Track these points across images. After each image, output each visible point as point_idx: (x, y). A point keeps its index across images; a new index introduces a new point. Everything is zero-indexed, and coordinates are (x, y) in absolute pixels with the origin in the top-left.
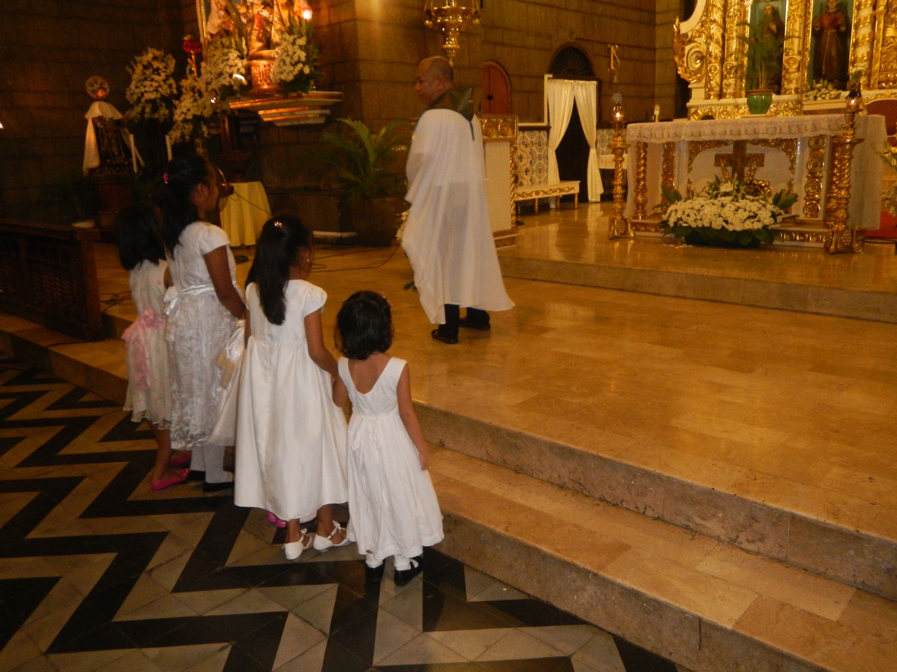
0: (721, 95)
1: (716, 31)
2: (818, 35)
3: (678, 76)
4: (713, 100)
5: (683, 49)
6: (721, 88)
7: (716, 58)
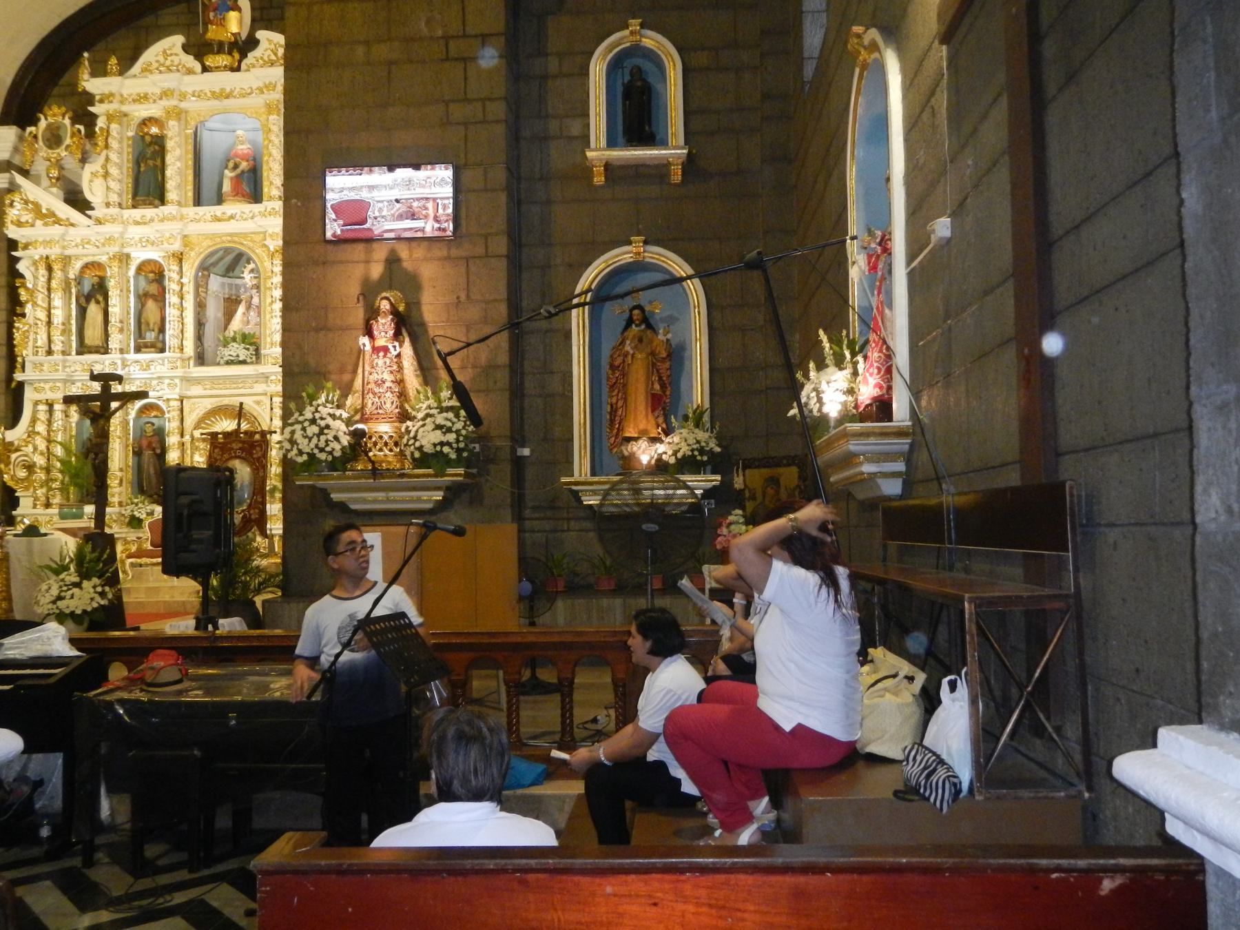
0: (48, 505)
1: (42, 445)
2: (138, 453)
3: (4, 483)
4: (40, 510)
6: (48, 499)
7: (41, 468)
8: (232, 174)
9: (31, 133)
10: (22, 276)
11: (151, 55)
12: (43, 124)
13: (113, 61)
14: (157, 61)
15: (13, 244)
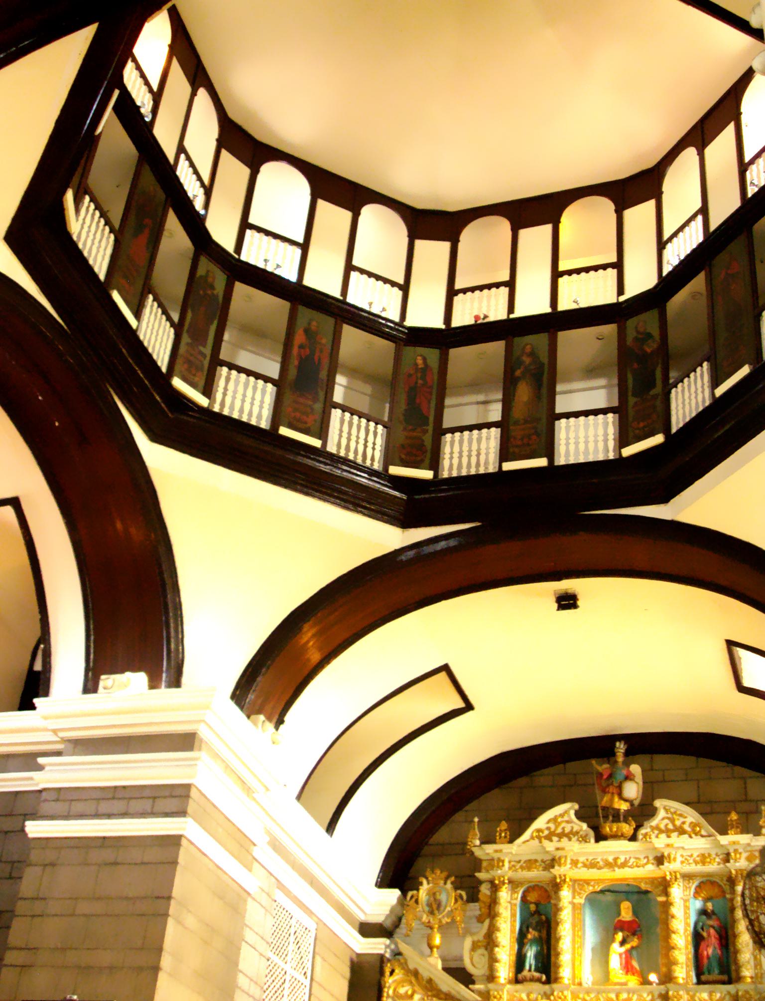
9: (412, 897)
11: (541, 822)
13: (504, 825)
14: (548, 828)
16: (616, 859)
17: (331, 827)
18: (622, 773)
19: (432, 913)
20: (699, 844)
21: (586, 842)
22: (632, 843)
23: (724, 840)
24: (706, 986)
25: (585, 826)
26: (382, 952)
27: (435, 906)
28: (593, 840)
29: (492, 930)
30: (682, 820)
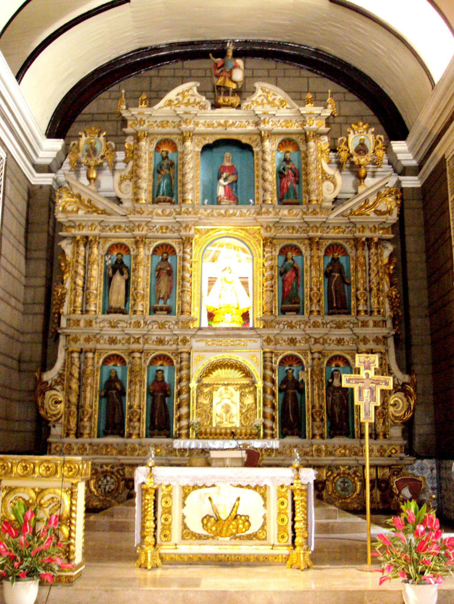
0: (79, 434)
5: (44, 394)
8: (226, 183)
9: (74, 144)
10: (63, 253)
11: (172, 95)
12: (83, 139)
15: (57, 226)
16: (226, 122)
17: (19, 77)
18: (230, 64)
19: (89, 156)
20: (284, 112)
21: (205, 109)
22: (238, 111)
23: (304, 111)
24: (287, 206)
25: (204, 98)
26: (50, 183)
27: (91, 152)
28: (210, 108)
29: (137, 166)
30: (273, 97)
